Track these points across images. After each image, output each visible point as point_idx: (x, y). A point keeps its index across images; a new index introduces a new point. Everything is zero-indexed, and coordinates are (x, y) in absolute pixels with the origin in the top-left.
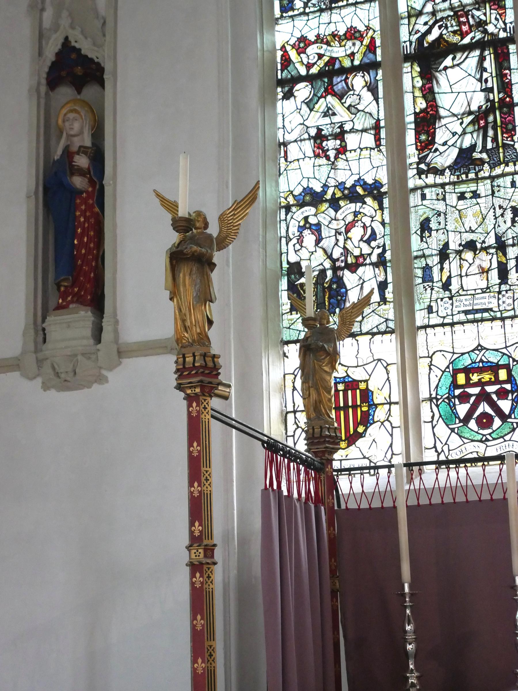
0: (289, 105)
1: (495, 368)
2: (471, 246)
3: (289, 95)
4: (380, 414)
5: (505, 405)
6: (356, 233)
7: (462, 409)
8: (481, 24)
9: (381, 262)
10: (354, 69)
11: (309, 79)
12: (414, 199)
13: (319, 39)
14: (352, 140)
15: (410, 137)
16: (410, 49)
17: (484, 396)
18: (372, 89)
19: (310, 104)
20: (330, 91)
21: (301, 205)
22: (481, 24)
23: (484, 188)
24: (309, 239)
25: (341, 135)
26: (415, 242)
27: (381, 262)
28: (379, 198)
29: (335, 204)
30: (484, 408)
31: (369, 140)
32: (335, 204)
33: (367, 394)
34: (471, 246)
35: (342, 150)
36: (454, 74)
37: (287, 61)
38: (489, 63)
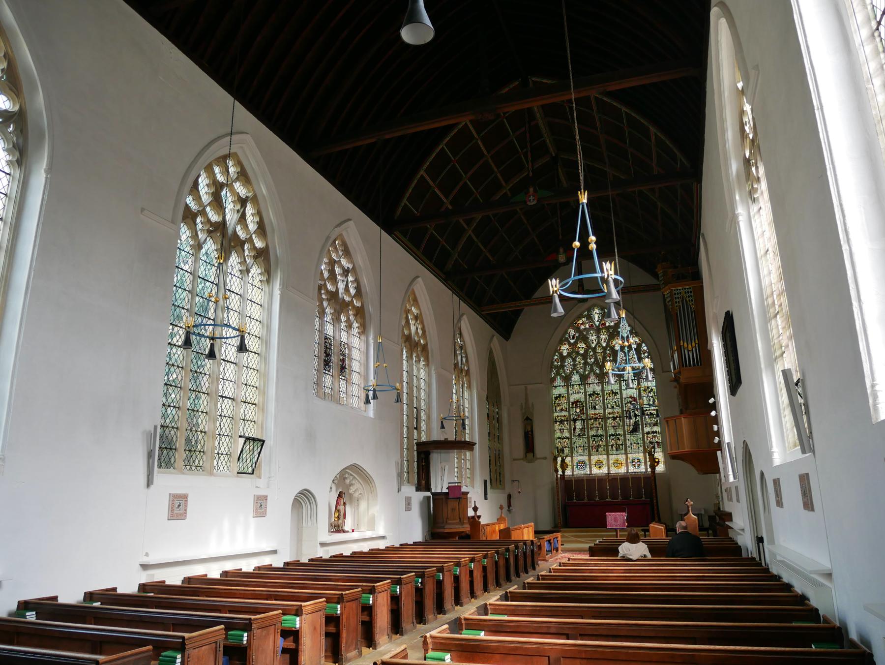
0: (555, 425)
1: (582, 462)
2: (580, 446)
3: (556, 423)
4: (569, 467)
5: (584, 467)
6: (565, 443)
7: (579, 467)
8: (581, 417)
9: (569, 447)
10: (565, 421)
11: (559, 421)
12: (573, 440)
13: (560, 416)
14: (565, 431)
15: (572, 431)
16: (572, 419)
17: (581, 465)
18: (567, 424)
19: (559, 425)
20: (562, 423)
21: (558, 439)
22: (581, 417)
23: (581, 439)
24: (559, 444)
25: (563, 430)
26: (573, 445)
27: (569, 447)
28: (568, 439)
29: (563, 439)
30: (581, 467)
31: (567, 431)
32: (563, 439)
33: (567, 464)
34: (580, 446)
35: (563, 432)
36: (578, 423)
37: (556, 419)
38: (582, 422)
